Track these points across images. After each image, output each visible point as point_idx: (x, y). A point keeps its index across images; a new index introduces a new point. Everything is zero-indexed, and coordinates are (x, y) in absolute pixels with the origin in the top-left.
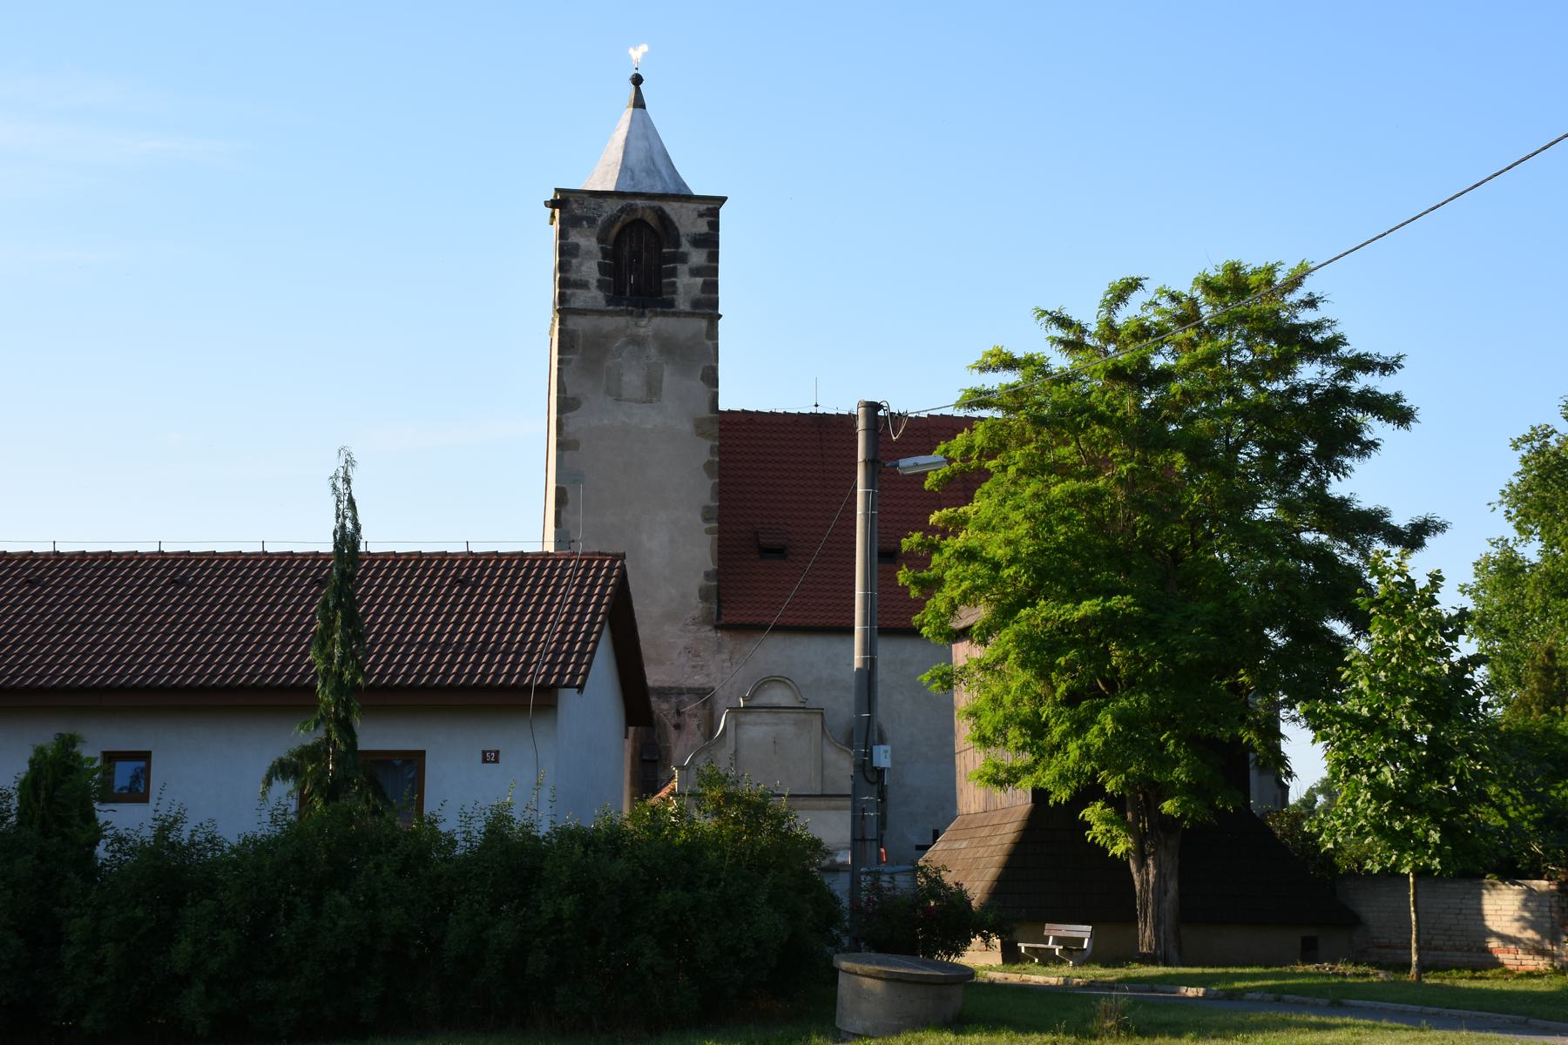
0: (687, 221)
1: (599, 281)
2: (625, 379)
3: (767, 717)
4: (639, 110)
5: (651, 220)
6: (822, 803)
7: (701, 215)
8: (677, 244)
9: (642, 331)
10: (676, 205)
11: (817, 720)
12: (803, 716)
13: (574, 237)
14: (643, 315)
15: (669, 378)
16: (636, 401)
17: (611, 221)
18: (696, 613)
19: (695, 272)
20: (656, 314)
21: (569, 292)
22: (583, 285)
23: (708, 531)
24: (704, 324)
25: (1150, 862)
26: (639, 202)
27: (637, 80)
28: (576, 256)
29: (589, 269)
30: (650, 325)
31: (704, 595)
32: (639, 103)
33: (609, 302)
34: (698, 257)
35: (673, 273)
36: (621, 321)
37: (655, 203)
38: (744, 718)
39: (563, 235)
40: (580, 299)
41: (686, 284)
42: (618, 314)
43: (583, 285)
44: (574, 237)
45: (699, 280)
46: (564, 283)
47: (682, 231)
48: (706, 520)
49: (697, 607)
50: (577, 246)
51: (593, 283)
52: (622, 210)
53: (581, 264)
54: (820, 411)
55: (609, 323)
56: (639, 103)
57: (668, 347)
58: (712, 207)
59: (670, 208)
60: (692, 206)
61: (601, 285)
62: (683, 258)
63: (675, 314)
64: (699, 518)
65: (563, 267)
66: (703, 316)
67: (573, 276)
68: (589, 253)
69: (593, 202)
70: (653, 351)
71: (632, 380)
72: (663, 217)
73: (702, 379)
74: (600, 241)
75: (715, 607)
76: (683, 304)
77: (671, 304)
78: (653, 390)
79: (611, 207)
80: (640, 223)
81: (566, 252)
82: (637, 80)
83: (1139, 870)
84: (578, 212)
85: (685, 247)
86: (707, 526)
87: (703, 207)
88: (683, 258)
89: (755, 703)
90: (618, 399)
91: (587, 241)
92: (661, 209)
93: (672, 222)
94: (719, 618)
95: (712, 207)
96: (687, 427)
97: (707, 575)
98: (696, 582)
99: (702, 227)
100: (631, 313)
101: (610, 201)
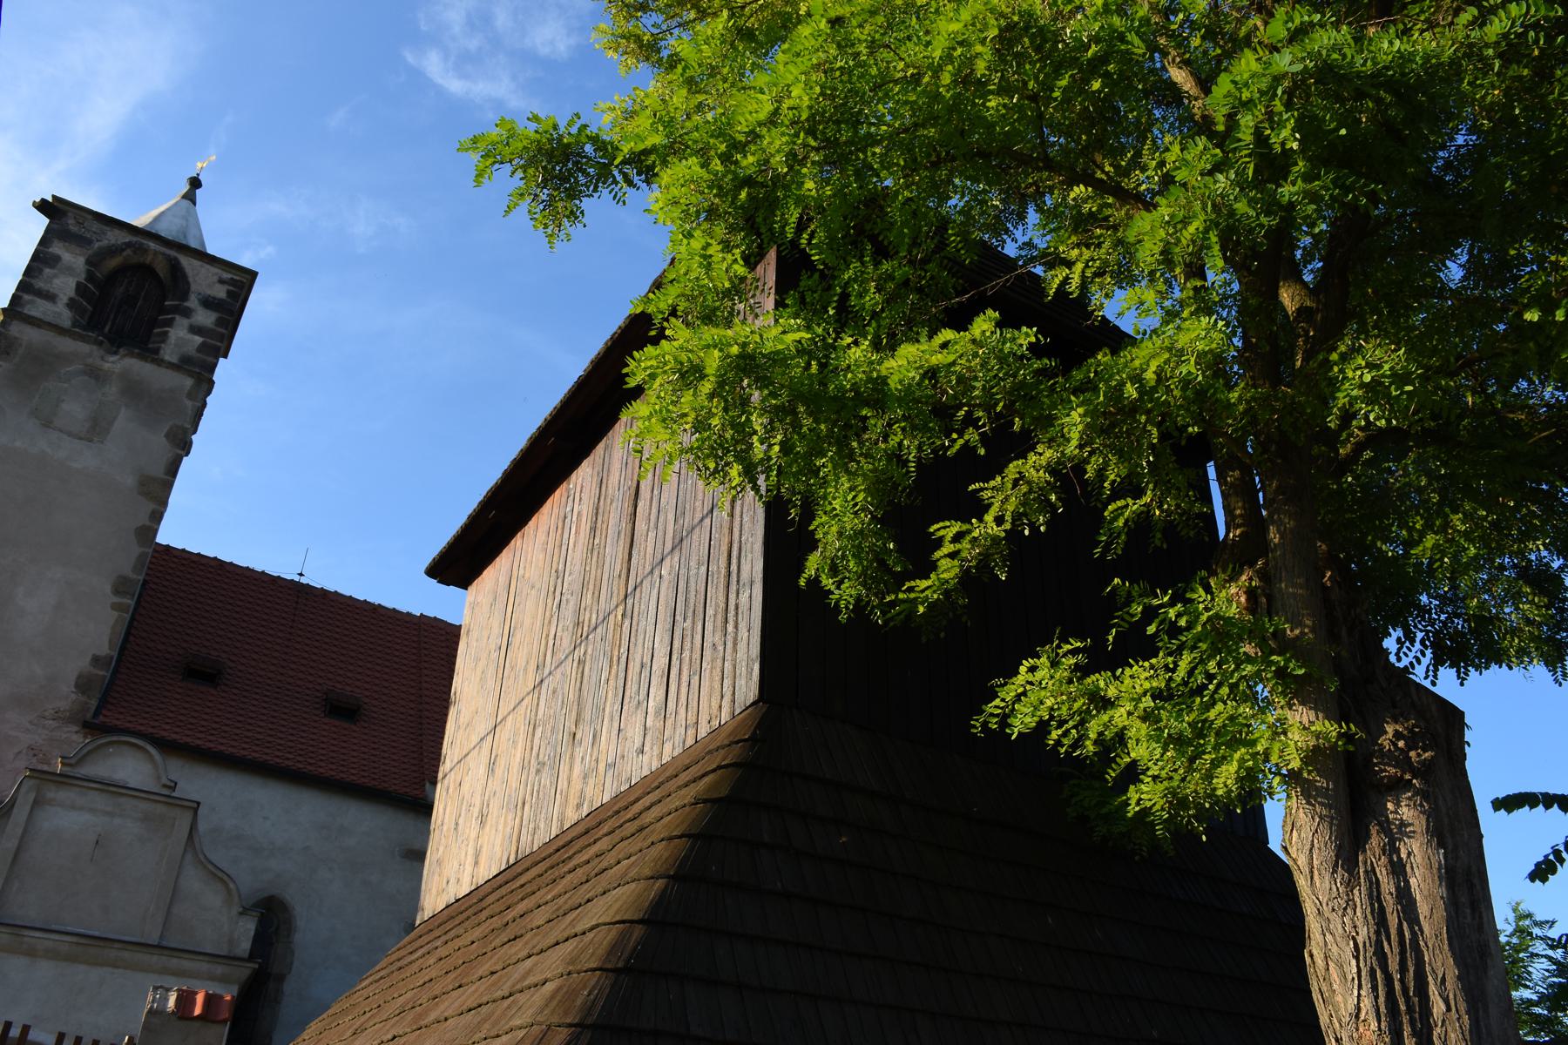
0: (203, 281)
1: (71, 299)
2: (65, 406)
3: (100, 800)
4: (187, 203)
5: (161, 269)
6: (154, 959)
7: (221, 281)
8: (185, 295)
9: (107, 366)
10: (196, 263)
11: (184, 820)
12: (160, 809)
13: (57, 248)
14: (115, 353)
15: (123, 421)
16: (70, 434)
17: (113, 251)
18: (64, 705)
19: (195, 330)
20: (132, 355)
21: (27, 297)
22: (51, 297)
23: (115, 607)
24: (189, 382)
25: (1406, 811)
26: (152, 245)
27: (195, 183)
28: (52, 267)
29: (65, 286)
30: (121, 364)
31: (83, 684)
32: (190, 197)
33: (75, 324)
34: (206, 318)
35: (170, 323)
36: (84, 348)
37: (173, 253)
38: (52, 793)
39: (44, 241)
40: (38, 308)
41: (180, 338)
42: (83, 339)
43: (51, 297)
44: (57, 248)
45: (198, 340)
46: (23, 287)
47: (193, 287)
48: (117, 591)
49: (66, 696)
50: (57, 259)
51: (63, 299)
52: (129, 245)
53: (55, 276)
54: (304, 580)
55: (67, 345)
56: (190, 197)
57: (134, 392)
58: (241, 282)
59: (186, 262)
60: (214, 270)
61: (72, 304)
62: (187, 313)
63: (160, 362)
64: (108, 589)
65: (29, 272)
66: (190, 374)
67: (39, 284)
68: (70, 270)
69: (96, 226)
70: (112, 390)
71: (75, 409)
72: (176, 269)
73: (167, 436)
74: (88, 262)
75: (94, 703)
76: (169, 353)
77: (157, 351)
78: (96, 429)
79: (114, 237)
80: (147, 271)
81: (41, 259)
82: (195, 183)
83: (1348, 853)
84: (74, 228)
85: (193, 302)
86: (116, 600)
87: (227, 276)
88: (187, 313)
89: (87, 770)
90: (47, 424)
91: (73, 259)
92: (176, 259)
93: (184, 276)
94: (96, 715)
95: (241, 282)
96: (130, 481)
97: (96, 660)
98: (76, 664)
99: (220, 292)
100: (100, 344)
101: (117, 232)
